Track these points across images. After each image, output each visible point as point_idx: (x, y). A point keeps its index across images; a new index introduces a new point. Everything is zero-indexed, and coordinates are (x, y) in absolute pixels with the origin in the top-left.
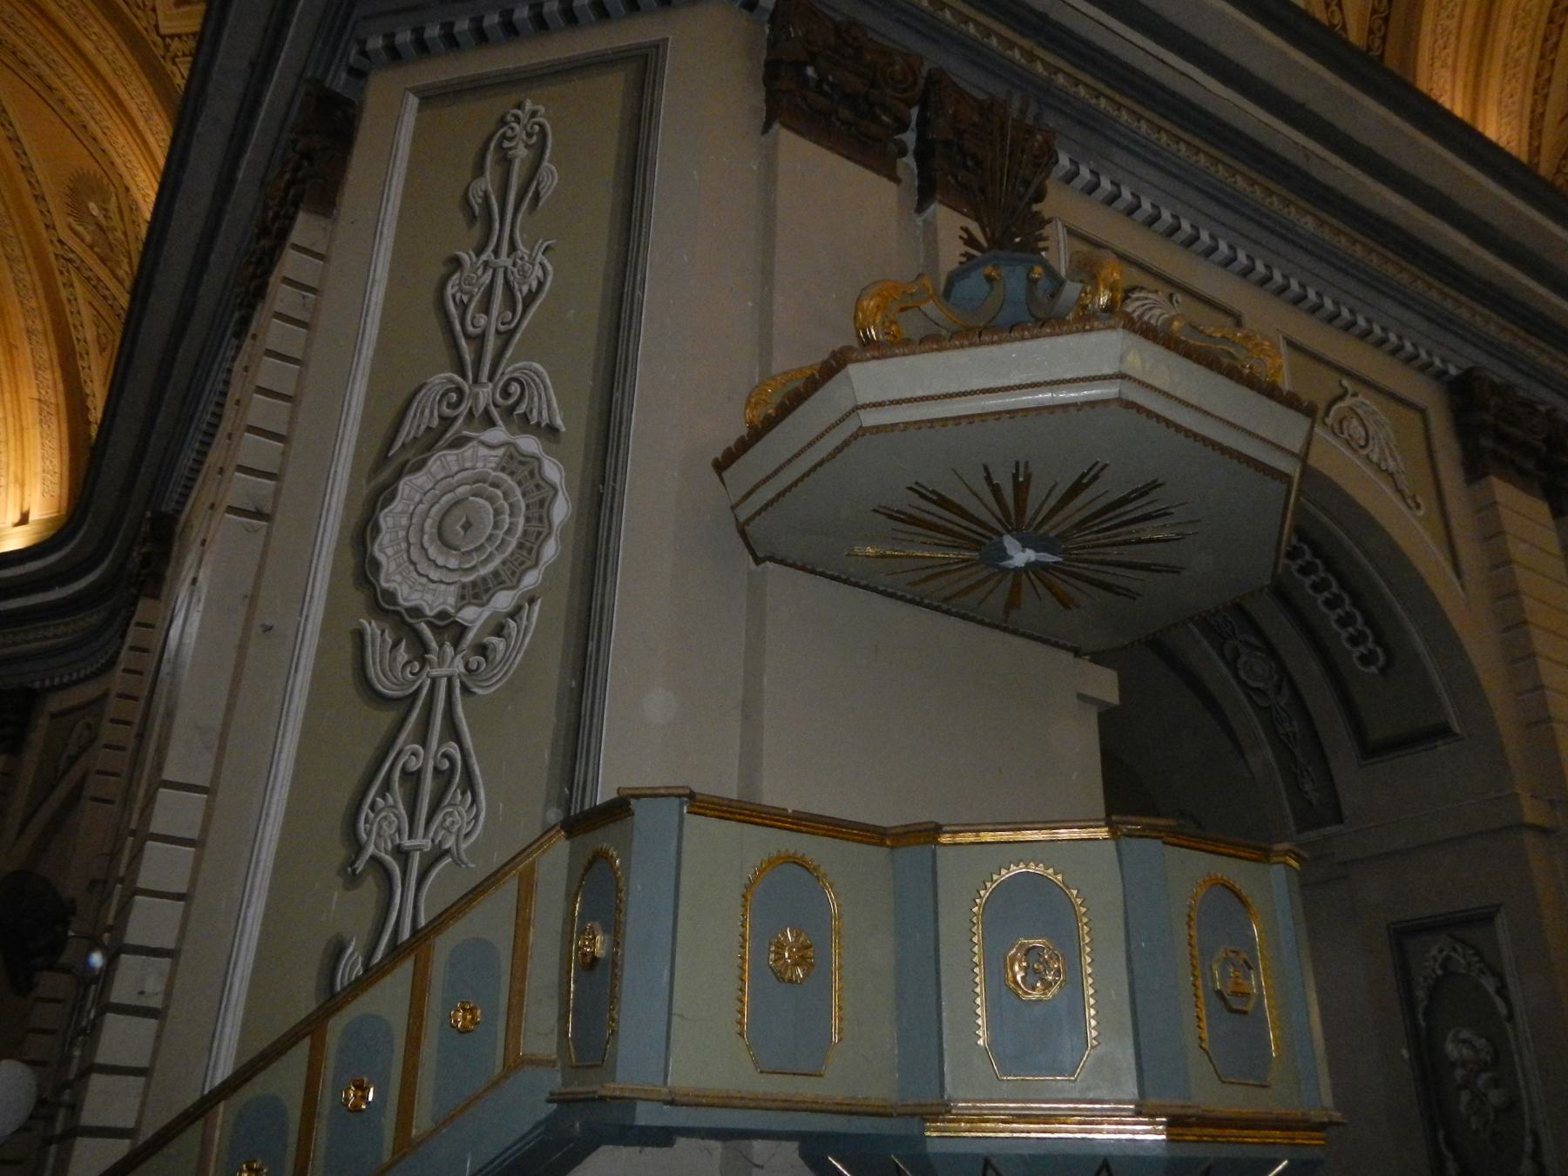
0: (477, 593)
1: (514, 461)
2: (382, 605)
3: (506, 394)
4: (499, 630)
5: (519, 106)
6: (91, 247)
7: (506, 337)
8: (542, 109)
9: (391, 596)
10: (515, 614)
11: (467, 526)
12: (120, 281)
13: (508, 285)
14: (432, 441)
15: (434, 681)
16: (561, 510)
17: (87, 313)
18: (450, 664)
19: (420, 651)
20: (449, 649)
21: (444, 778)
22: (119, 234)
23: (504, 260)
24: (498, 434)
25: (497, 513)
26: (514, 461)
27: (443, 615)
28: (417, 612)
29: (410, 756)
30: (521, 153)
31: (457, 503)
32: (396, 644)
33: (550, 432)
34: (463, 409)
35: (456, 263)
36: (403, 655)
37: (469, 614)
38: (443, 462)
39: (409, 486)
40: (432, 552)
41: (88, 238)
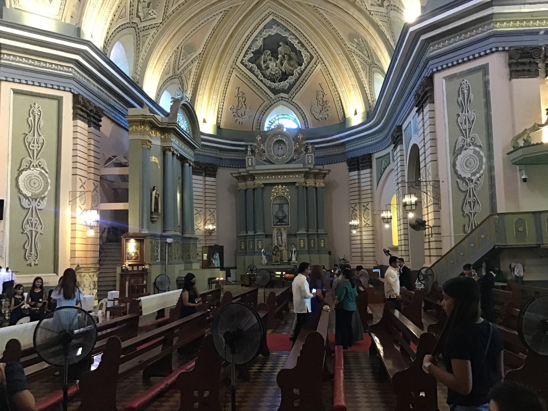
0: (474, 174)
1: (475, 152)
2: (459, 177)
3: (472, 140)
4: (478, 180)
5: (463, 81)
6: (356, 48)
7: (470, 129)
8: (468, 81)
9: (460, 175)
10: (480, 177)
11: (470, 163)
12: (366, 55)
13: (468, 119)
14: (462, 149)
15: (470, 188)
16: (484, 160)
17: (358, 62)
18: (472, 186)
19: (467, 184)
20: (471, 183)
21: (474, 202)
22: (363, 45)
23: (467, 114)
24: (472, 147)
25: (474, 161)
26: (475, 152)
27: (469, 178)
28: (465, 178)
29: (468, 199)
30: (466, 91)
31: (468, 159)
32: (463, 183)
33: (480, 147)
34: (465, 143)
35: (458, 115)
36: (464, 184)
37: (473, 178)
38: (464, 152)
39: (459, 157)
40: (465, 168)
41: (355, 46)
